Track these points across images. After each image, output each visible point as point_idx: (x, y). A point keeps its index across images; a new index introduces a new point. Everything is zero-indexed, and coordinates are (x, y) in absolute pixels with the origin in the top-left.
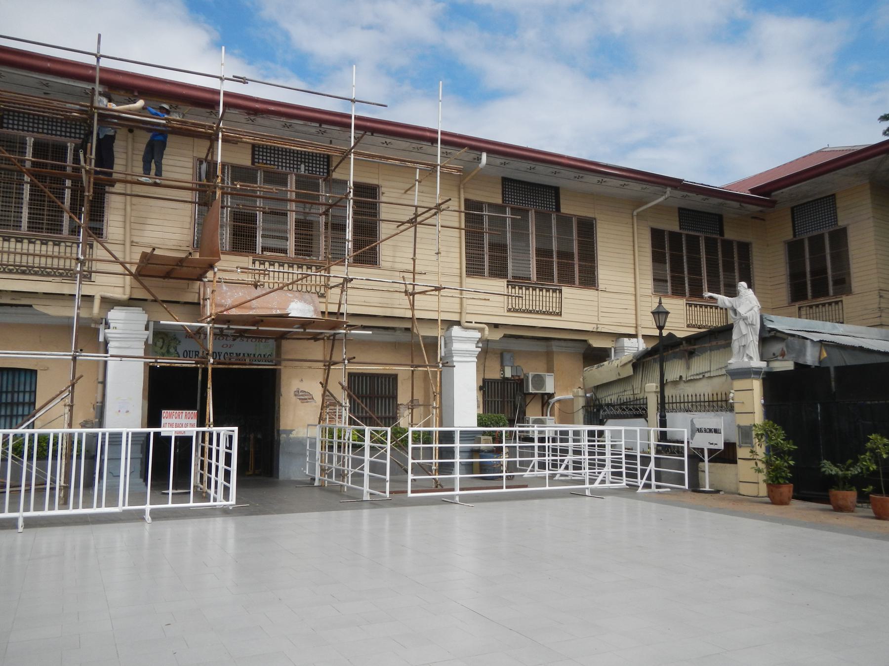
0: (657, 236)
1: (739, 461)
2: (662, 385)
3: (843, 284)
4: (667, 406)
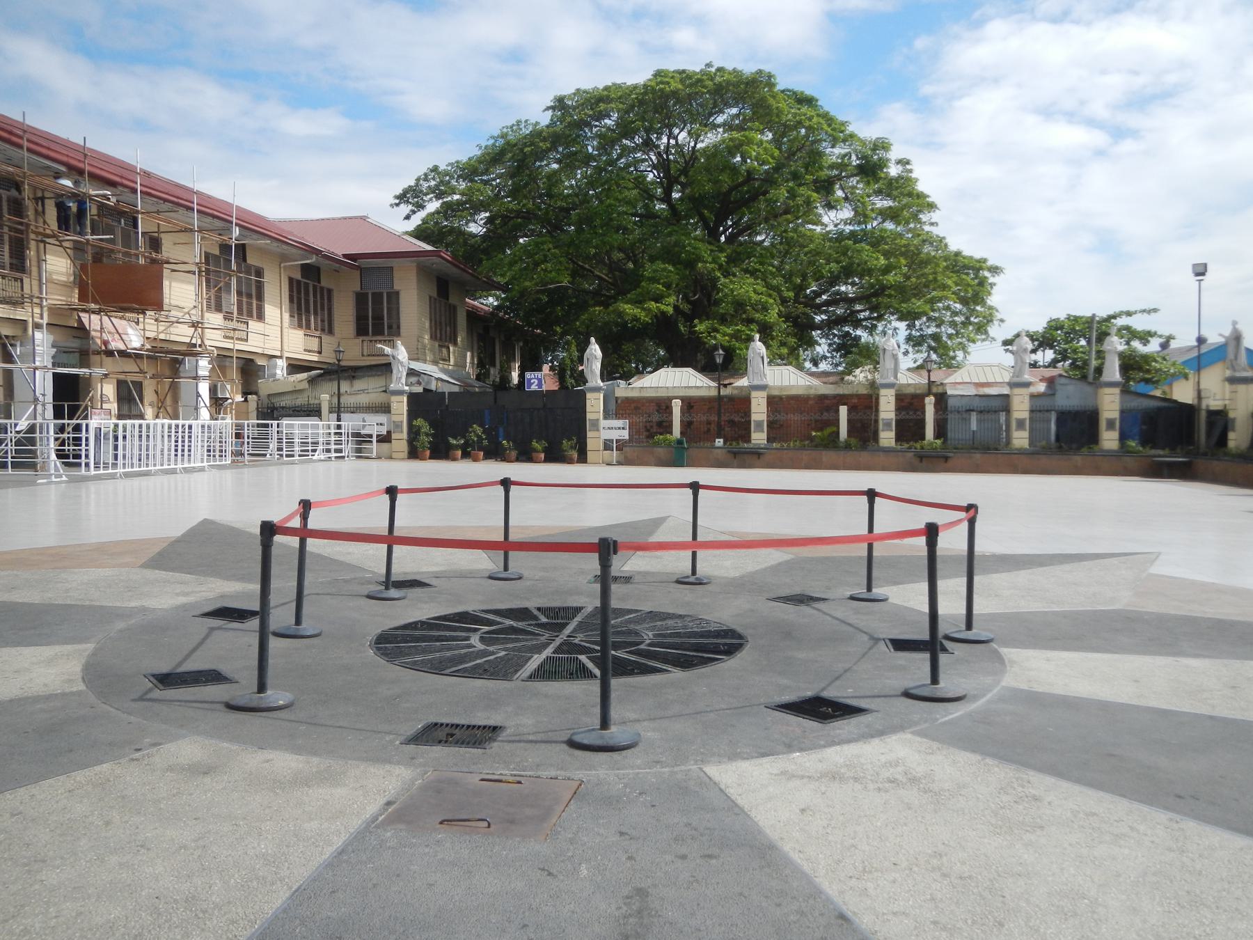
0: (291, 280)
4: (342, 409)
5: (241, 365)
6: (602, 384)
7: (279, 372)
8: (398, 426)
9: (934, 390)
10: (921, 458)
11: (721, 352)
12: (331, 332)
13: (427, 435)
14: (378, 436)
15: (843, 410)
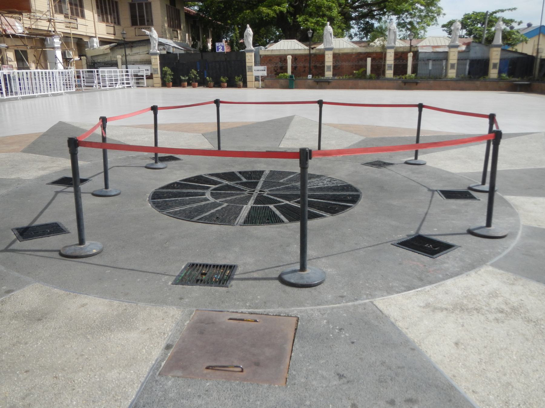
4: (128, 63)
5: (76, 42)
6: (253, 48)
7: (95, 44)
8: (155, 70)
9: (413, 50)
11: (311, 31)
12: (119, 24)
13: (170, 75)
14: (146, 76)
15: (369, 60)
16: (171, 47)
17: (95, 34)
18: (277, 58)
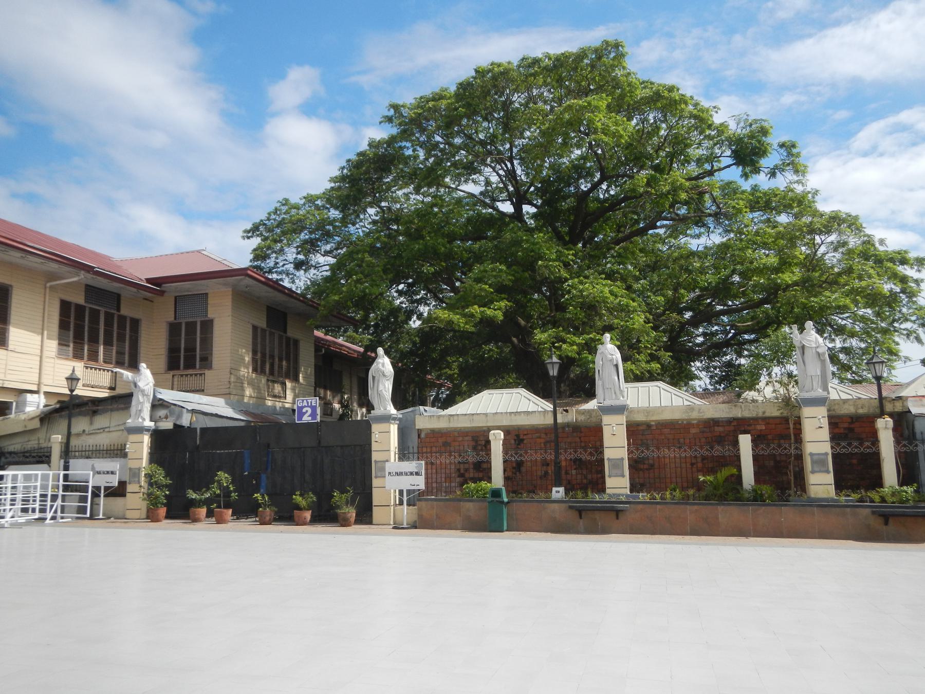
0: (65, 306)
1: (128, 495)
2: (69, 435)
3: (206, 362)
6: (393, 411)
8: (135, 473)
9: (889, 407)
10: (886, 518)
15: (745, 441)
16: (185, 411)
17: (39, 385)
18: (467, 438)
